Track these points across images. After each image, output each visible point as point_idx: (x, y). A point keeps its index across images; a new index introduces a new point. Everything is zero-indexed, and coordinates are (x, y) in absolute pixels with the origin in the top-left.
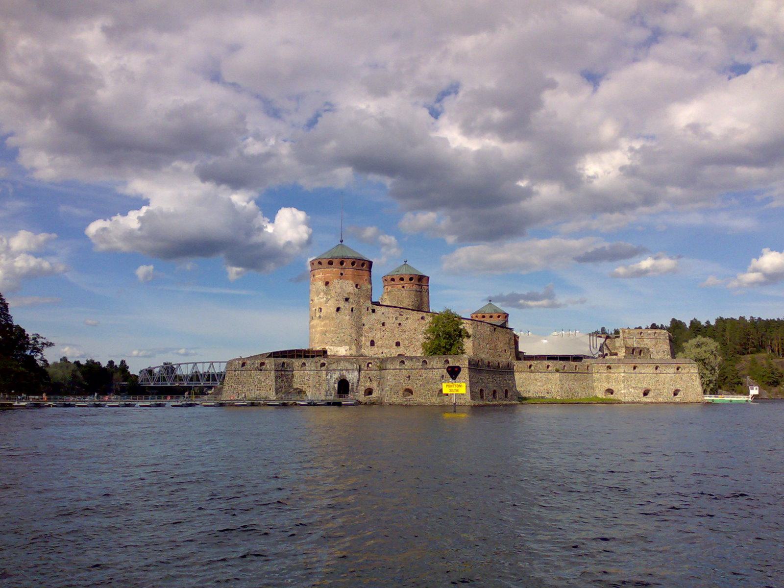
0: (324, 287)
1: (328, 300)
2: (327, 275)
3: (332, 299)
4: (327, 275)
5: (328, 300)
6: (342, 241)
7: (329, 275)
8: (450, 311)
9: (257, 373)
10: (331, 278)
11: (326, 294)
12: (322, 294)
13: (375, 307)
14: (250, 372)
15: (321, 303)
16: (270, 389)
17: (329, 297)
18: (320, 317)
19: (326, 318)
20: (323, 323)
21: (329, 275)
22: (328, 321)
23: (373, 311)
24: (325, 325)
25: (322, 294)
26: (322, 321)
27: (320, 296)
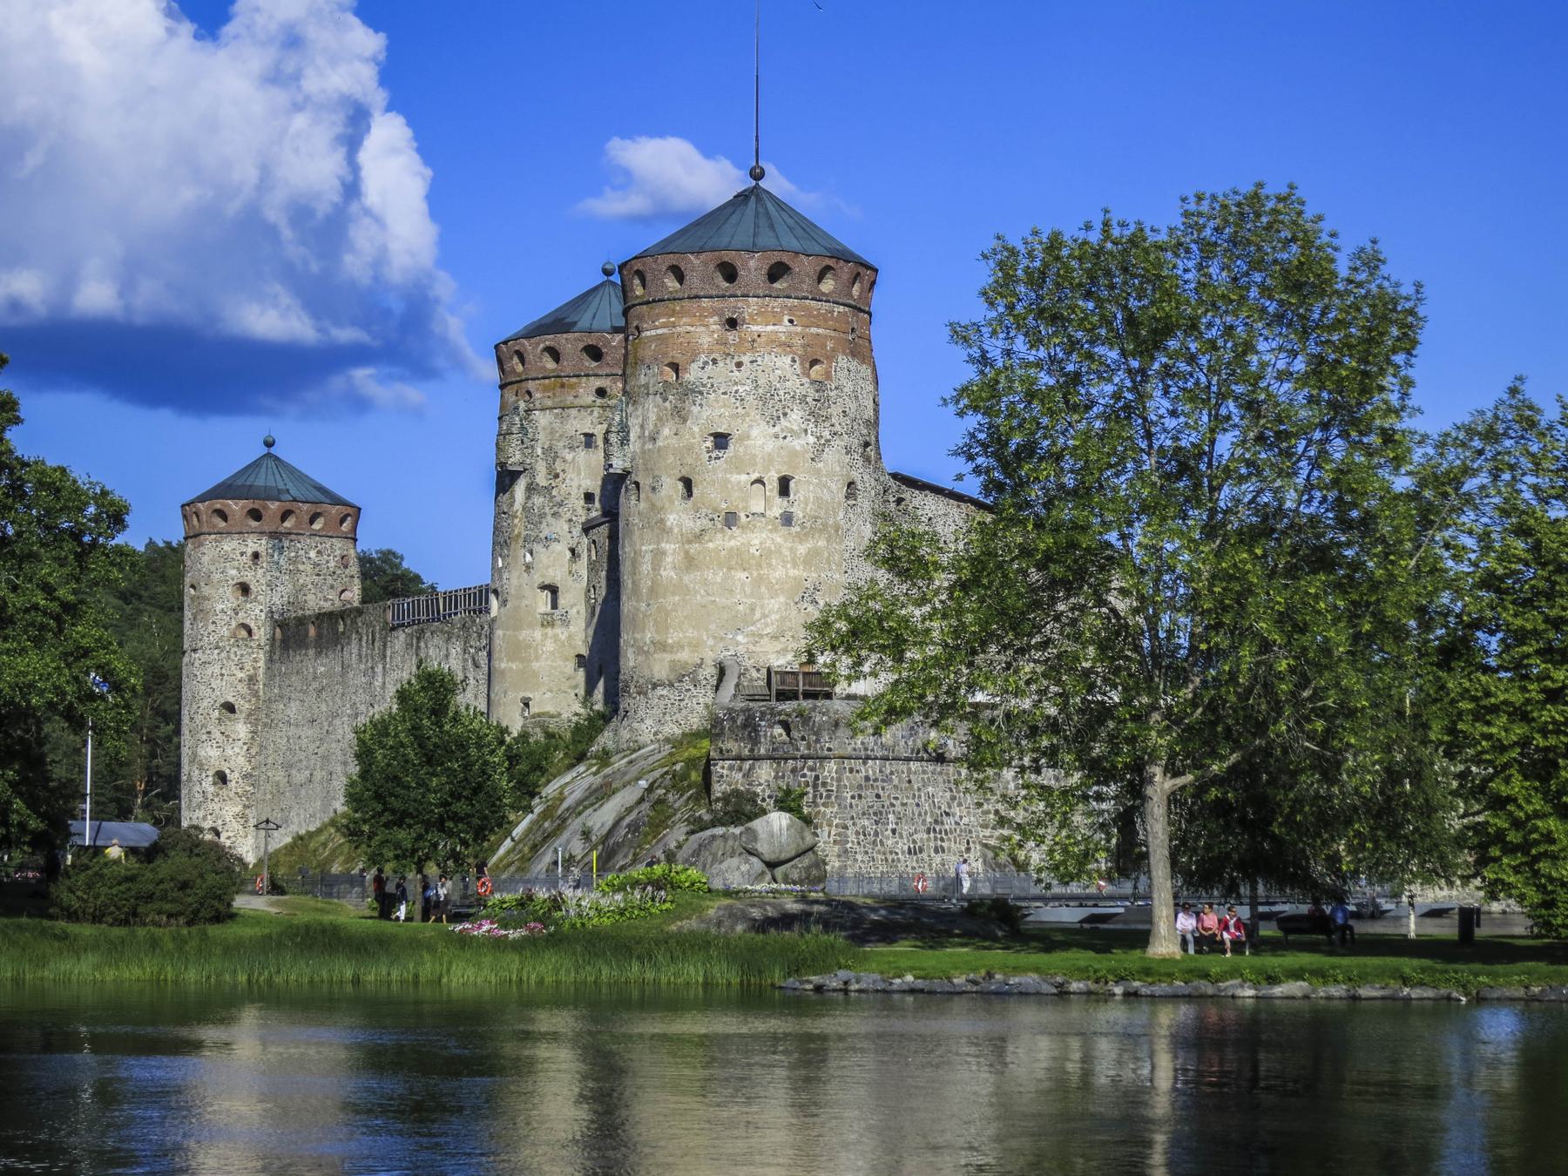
1: (821, 447)
2: (814, 330)
3: (839, 443)
4: (814, 330)
5: (821, 447)
7: (820, 331)
8: (43, 463)
9: (924, 772)
10: (830, 345)
11: (816, 415)
13: (907, 493)
14: (905, 768)
15: (794, 454)
16: (968, 850)
17: (826, 434)
18: (787, 519)
19: (816, 526)
20: (802, 549)
21: (820, 331)
24: (809, 560)
25: (796, 417)
26: (801, 538)
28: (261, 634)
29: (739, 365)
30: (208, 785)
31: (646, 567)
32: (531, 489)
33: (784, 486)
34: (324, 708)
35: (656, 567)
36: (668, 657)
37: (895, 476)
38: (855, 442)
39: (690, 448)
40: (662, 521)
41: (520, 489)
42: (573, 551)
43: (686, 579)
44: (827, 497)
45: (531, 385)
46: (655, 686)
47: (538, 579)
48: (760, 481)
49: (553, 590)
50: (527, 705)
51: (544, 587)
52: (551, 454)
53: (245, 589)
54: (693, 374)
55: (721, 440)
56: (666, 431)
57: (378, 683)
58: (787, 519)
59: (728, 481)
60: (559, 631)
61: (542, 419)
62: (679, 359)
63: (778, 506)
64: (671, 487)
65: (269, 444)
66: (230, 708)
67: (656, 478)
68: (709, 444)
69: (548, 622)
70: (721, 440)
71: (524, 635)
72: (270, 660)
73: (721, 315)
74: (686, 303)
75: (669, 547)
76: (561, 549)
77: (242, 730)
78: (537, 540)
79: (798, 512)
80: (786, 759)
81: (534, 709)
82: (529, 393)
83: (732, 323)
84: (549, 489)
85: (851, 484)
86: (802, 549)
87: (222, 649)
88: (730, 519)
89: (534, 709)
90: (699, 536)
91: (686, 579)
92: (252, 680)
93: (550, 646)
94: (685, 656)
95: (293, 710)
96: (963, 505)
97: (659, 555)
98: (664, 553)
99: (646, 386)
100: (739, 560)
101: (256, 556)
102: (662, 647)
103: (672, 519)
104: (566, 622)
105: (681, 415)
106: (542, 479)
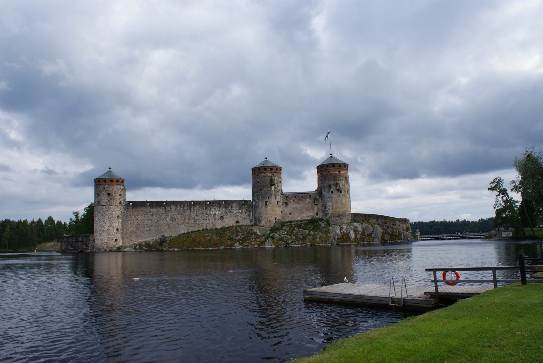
6: (331, 154)
30: (115, 231)
31: (344, 201)
32: (275, 188)
34: (155, 217)
41: (273, 188)
47: (277, 200)
49: (278, 202)
50: (276, 219)
53: (120, 195)
57: (188, 212)
65: (110, 169)
66: (118, 217)
69: (279, 207)
77: (121, 221)
95: (139, 218)
97: (346, 200)
106: (276, 187)
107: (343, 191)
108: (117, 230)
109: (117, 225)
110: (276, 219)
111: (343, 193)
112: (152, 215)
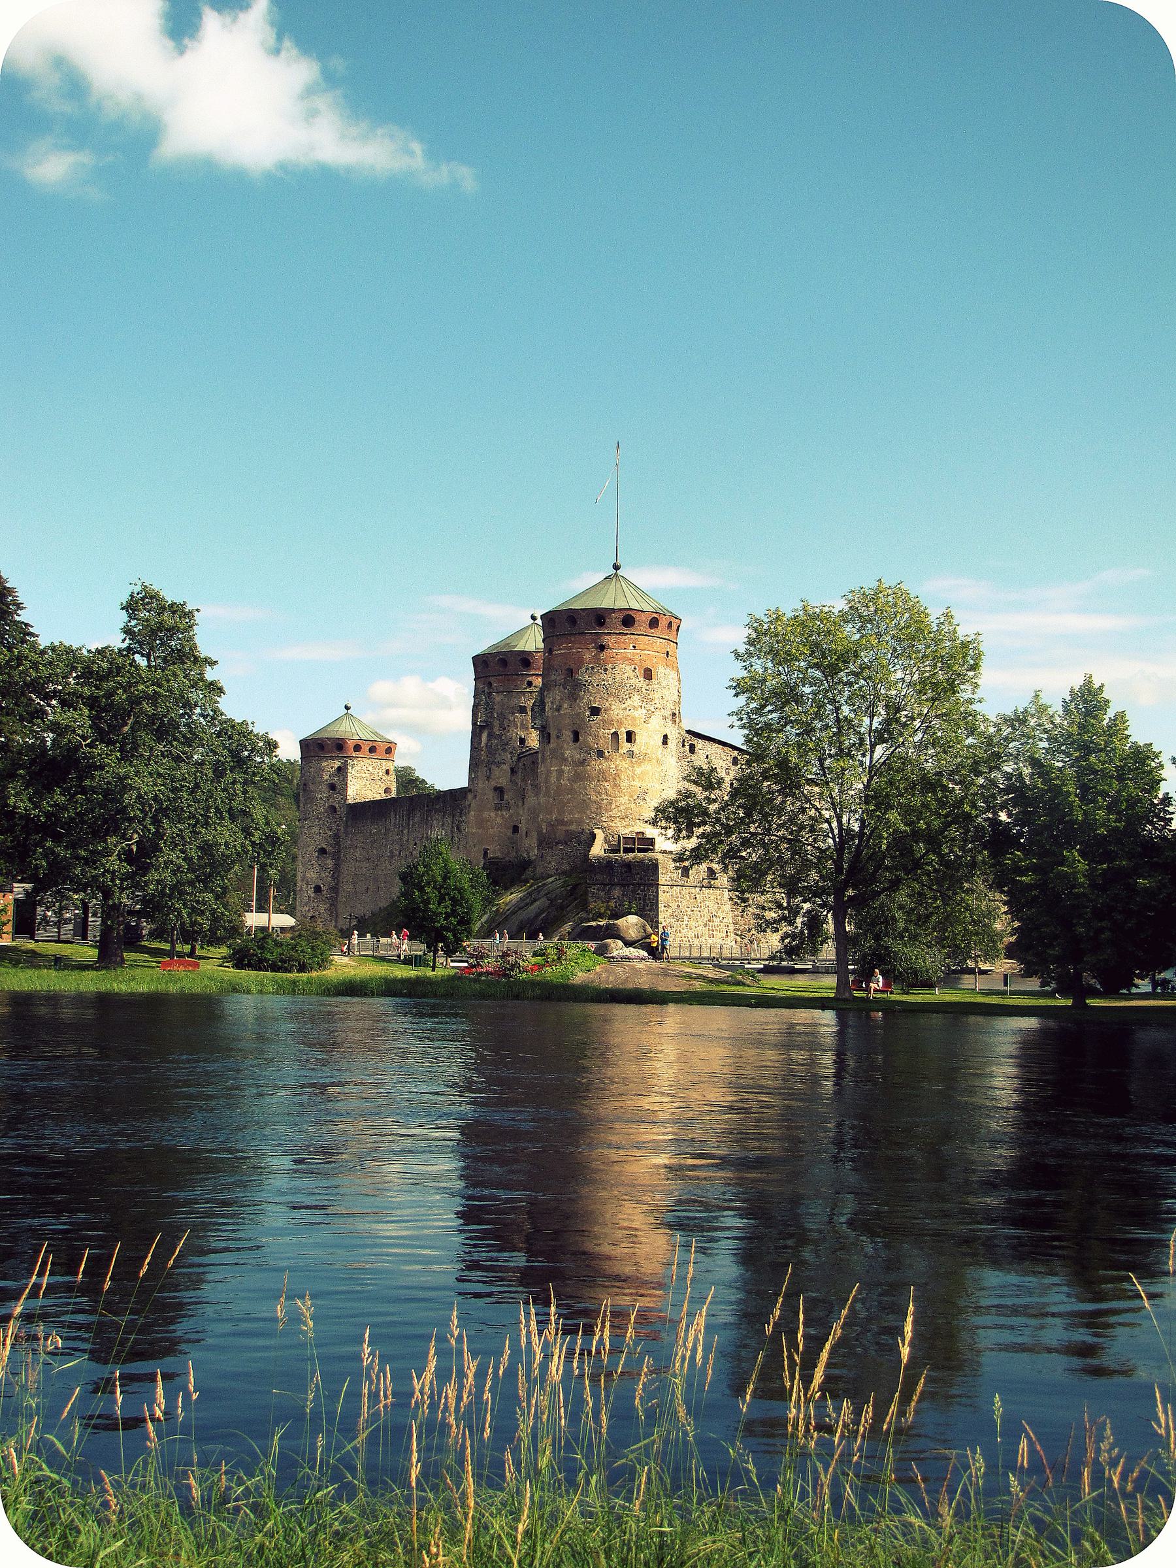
0: (641, 683)
3: (658, 713)
6: (616, 567)
12: (636, 699)
13: (695, 741)
15: (634, 719)
22: (649, 767)
23: (692, 749)
26: (640, 764)
27: (629, 702)
28: (342, 812)
29: (606, 670)
30: (311, 892)
31: (553, 780)
32: (490, 736)
33: (630, 736)
35: (559, 780)
36: (564, 828)
37: (688, 732)
38: (668, 713)
39: (578, 714)
40: (563, 754)
42: (512, 769)
43: (575, 786)
44: (652, 743)
45: (492, 679)
46: (557, 843)
47: (493, 784)
48: (616, 734)
49: (500, 791)
50: (486, 854)
51: (496, 789)
52: (502, 717)
53: (332, 787)
54: (582, 676)
55: (595, 711)
56: (566, 706)
58: (631, 754)
59: (596, 736)
60: (506, 814)
61: (498, 698)
62: (573, 666)
63: (625, 746)
64: (567, 735)
65: (347, 708)
66: (323, 851)
67: (560, 731)
68: (588, 713)
69: (498, 808)
70: (595, 711)
71: (486, 814)
72: (347, 826)
73: (596, 643)
74: (578, 637)
75: (566, 769)
76: (506, 767)
77: (330, 863)
78: (493, 763)
79: (636, 751)
80: (628, 885)
81: (490, 855)
82: (490, 684)
83: (602, 648)
84: (500, 736)
85: (665, 737)
86: (638, 770)
87: (320, 819)
88: (600, 754)
89: (490, 855)
90: (583, 762)
91: (575, 786)
92: (336, 836)
93: (499, 821)
94: (573, 827)
95: (358, 854)
96: (726, 748)
97: (560, 773)
98: (563, 771)
99: (555, 681)
100: (603, 776)
101: (339, 769)
102: (561, 822)
103: (567, 753)
104: (508, 808)
105: (574, 697)
107: (553, 733)
108: (318, 889)
109: (314, 876)
110: (486, 854)
111: (551, 746)
112: (373, 842)
